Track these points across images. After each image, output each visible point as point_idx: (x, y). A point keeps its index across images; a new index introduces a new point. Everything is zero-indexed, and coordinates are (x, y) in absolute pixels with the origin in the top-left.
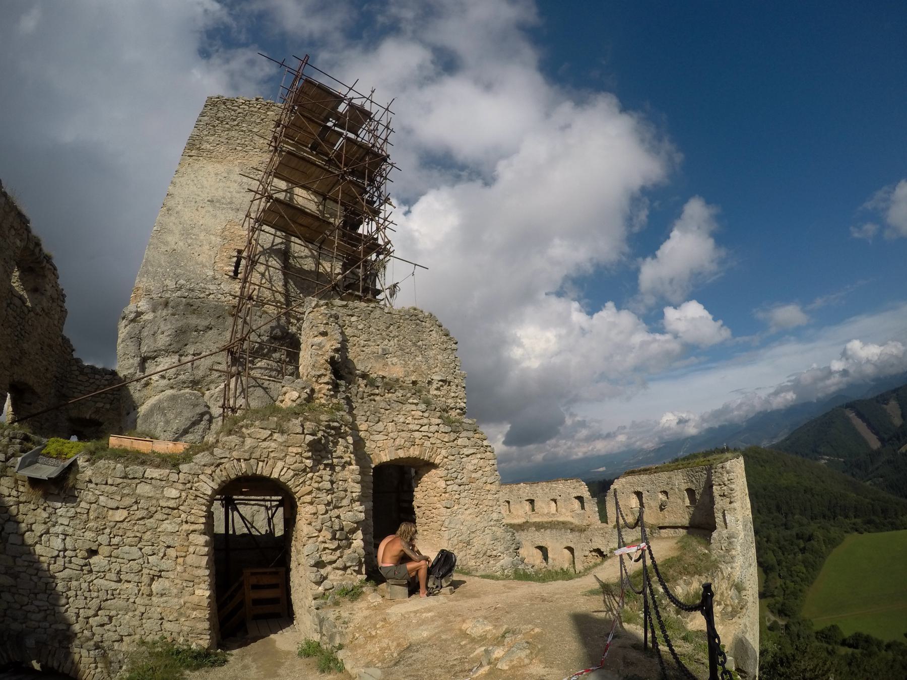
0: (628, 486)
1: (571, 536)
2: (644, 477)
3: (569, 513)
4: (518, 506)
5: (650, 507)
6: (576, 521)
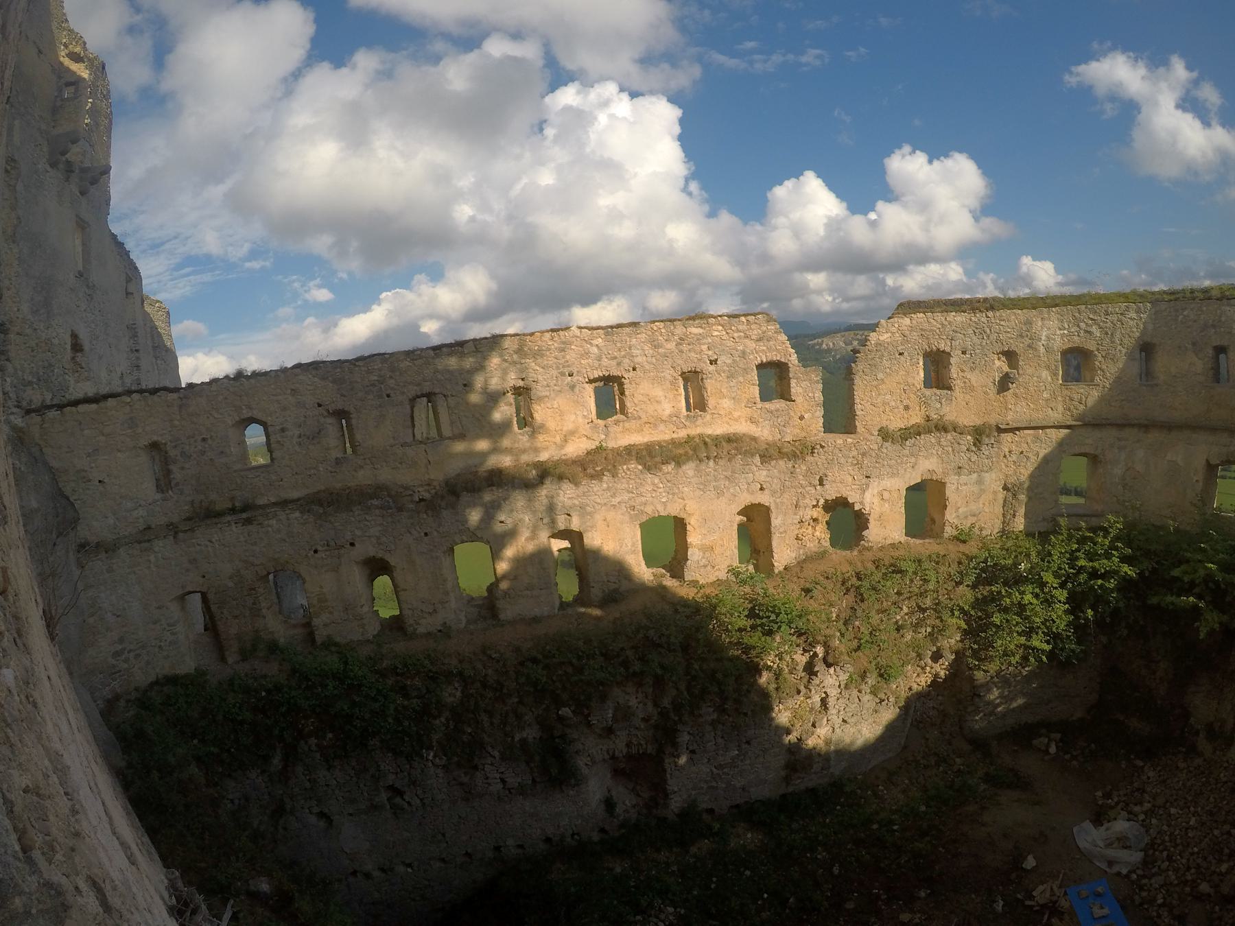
1: (762, 475)
2: (959, 318)
3: (734, 411)
4: (560, 402)
6: (764, 432)
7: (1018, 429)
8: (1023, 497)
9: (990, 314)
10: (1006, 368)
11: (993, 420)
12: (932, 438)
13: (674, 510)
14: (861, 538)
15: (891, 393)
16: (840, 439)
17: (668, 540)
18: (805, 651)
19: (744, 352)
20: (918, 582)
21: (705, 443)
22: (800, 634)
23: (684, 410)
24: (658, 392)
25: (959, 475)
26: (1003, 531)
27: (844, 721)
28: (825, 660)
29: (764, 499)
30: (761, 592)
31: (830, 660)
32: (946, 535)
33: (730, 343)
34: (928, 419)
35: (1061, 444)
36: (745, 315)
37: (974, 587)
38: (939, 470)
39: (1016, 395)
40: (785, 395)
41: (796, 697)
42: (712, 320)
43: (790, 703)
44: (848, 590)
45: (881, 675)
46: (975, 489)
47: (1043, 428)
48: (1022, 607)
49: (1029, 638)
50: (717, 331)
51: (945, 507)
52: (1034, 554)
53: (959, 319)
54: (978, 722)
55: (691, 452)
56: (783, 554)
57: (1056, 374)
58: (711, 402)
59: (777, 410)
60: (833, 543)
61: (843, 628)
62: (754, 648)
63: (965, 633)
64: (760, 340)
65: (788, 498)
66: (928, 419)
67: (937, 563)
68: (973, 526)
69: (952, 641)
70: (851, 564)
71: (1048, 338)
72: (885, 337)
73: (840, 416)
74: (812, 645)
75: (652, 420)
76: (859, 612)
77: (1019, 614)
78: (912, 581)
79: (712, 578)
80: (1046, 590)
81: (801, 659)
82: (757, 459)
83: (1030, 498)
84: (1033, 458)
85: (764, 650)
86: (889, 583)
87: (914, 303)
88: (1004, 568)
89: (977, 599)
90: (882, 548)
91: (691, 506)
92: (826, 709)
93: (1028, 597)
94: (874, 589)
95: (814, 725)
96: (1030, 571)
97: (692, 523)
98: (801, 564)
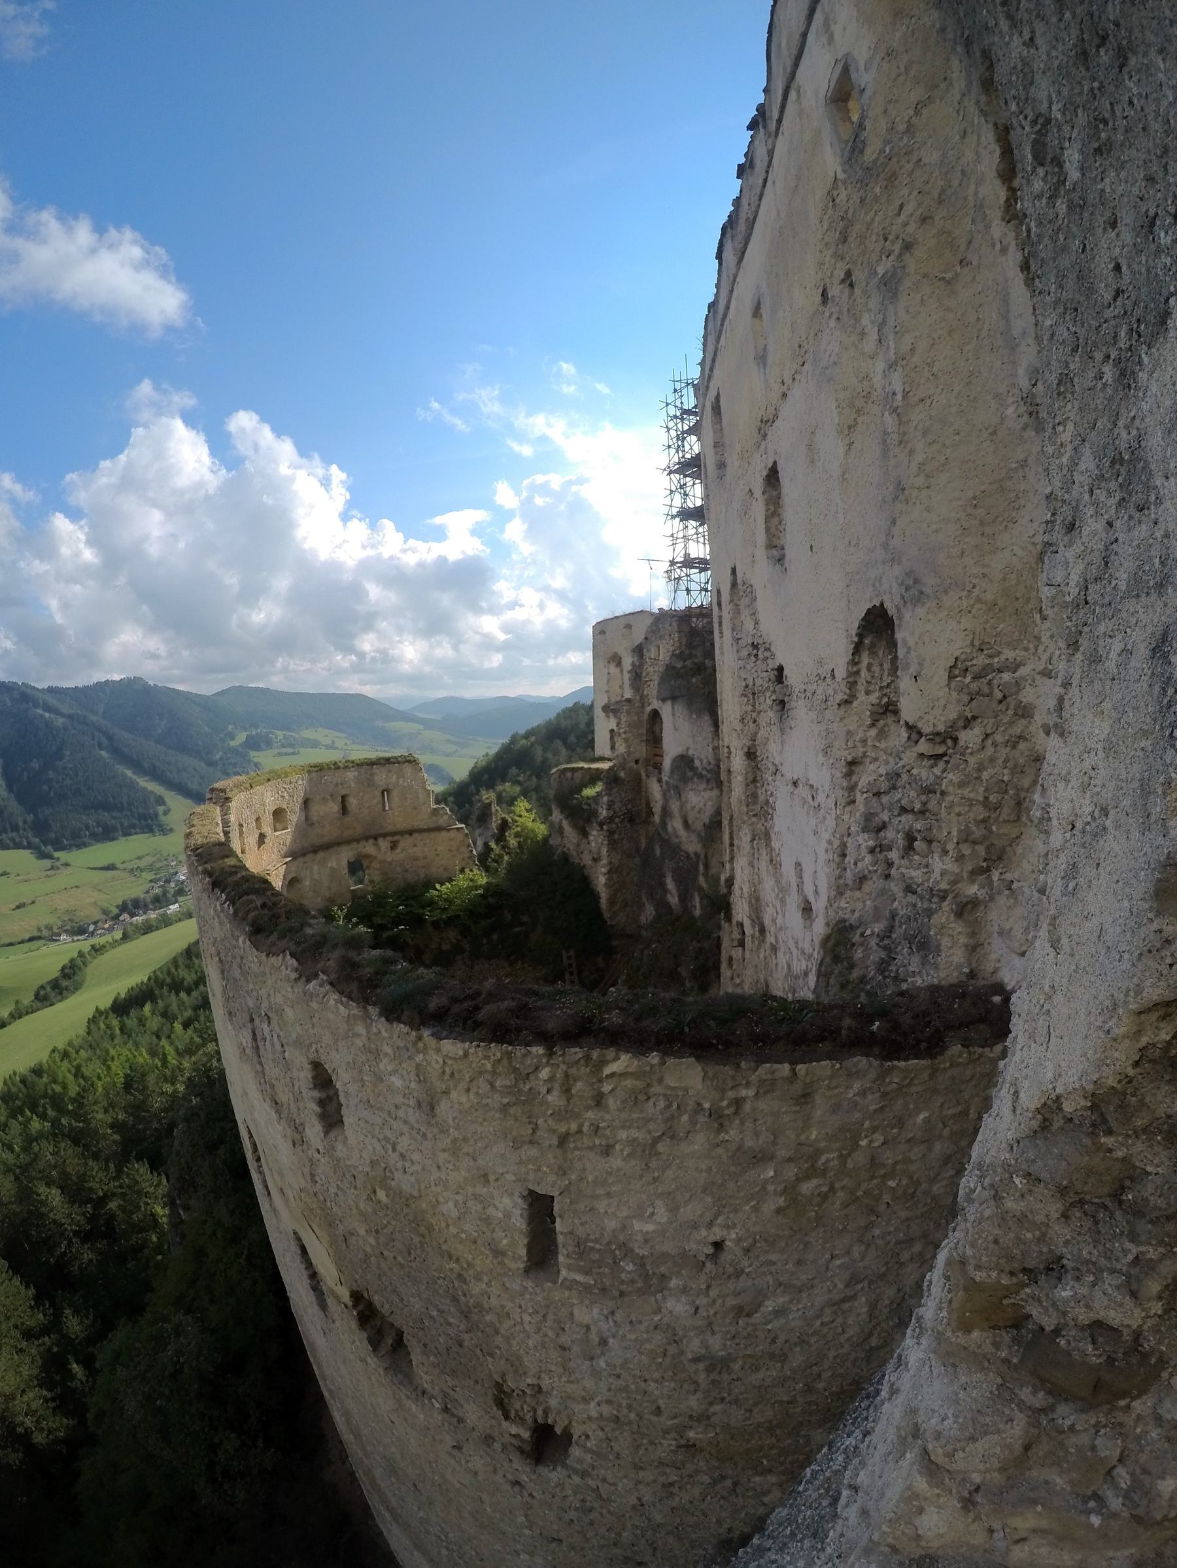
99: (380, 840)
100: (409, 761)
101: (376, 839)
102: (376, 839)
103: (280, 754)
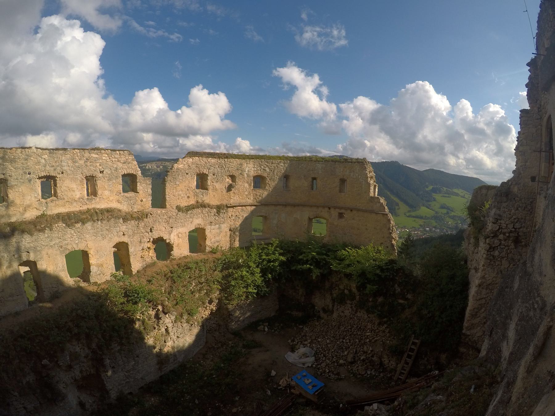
0: (194, 166)
1: (124, 228)
2: (213, 161)
3: (110, 197)
5: (215, 189)
6: (124, 207)
7: (235, 206)
8: (237, 233)
9: (226, 160)
10: (231, 182)
11: (225, 202)
12: (199, 210)
13: (82, 247)
14: (171, 255)
15: (182, 191)
16: (159, 211)
17: (80, 261)
18: (153, 309)
19: (116, 168)
20: (197, 272)
21: (96, 213)
22: (150, 302)
23: (86, 195)
24: (74, 186)
25: (211, 225)
26: (230, 247)
27: (177, 337)
28: (163, 312)
29: (125, 239)
30: (128, 284)
31: (166, 311)
32: (207, 251)
33: (110, 164)
34: (197, 202)
35: (252, 212)
36: (119, 150)
37: (221, 271)
38: (202, 224)
39: (234, 193)
40: (135, 190)
41: (154, 331)
42: (103, 151)
43: (152, 334)
44: (168, 279)
45: (189, 314)
46: (218, 231)
47: (245, 206)
48: (242, 277)
49: (247, 289)
50: (105, 157)
51: (206, 239)
52: (244, 255)
53: (213, 161)
54: (233, 326)
55: (89, 217)
56: (136, 265)
57: (250, 185)
58: (99, 192)
59: (131, 197)
60: (158, 258)
61: (168, 296)
62: (130, 311)
63: (221, 290)
64: (124, 163)
65: (136, 238)
66: (197, 202)
67: (205, 263)
68: (218, 246)
69: (216, 295)
70: (167, 267)
71: (248, 171)
72: (181, 166)
73: (159, 200)
74: (156, 306)
75: (70, 200)
76: (174, 288)
77: (242, 280)
78: (195, 271)
79: (104, 280)
80: (251, 269)
81: (152, 313)
82: (121, 220)
83: (240, 234)
84: (241, 218)
85: (135, 312)
86: (185, 274)
87: (194, 152)
88: (232, 263)
89: (223, 276)
90: (180, 259)
91: (91, 244)
92: (169, 333)
93: (244, 273)
94: (179, 277)
95: (165, 342)
96: (243, 262)
97: (91, 253)
98: (145, 269)
99: (332, 210)
100: (358, 162)
101: (329, 208)
102: (329, 208)
103: (444, 196)
